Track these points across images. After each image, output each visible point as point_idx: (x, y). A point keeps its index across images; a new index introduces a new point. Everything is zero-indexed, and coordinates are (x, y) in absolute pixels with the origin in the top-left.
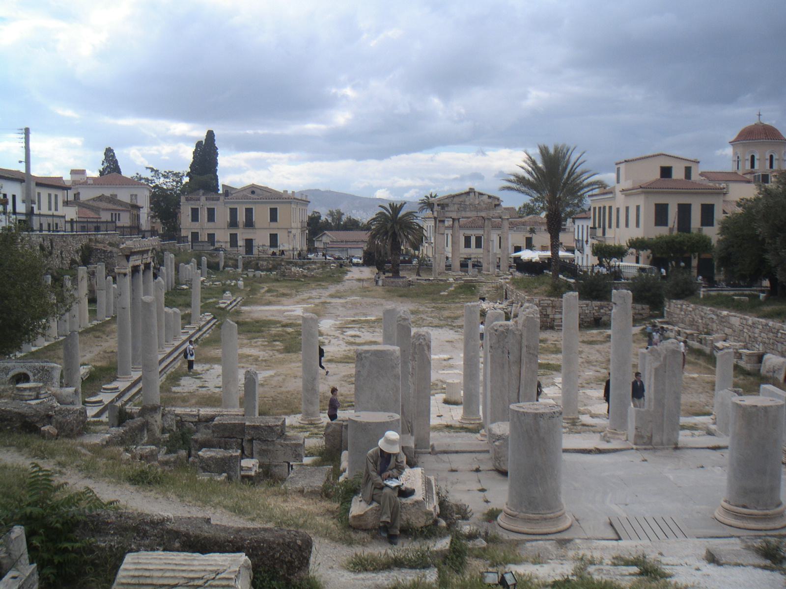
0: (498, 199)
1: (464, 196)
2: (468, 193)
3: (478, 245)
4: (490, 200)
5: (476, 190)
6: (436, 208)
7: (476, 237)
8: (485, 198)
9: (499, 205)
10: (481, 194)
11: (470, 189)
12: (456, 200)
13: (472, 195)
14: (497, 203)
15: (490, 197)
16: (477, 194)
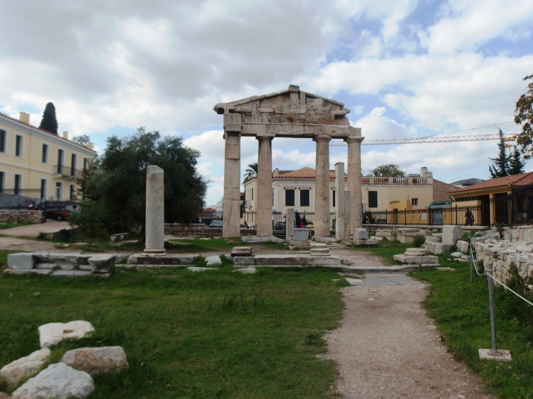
0: (341, 106)
1: (280, 100)
2: (286, 95)
3: (305, 201)
4: (327, 108)
5: (301, 89)
7: (301, 191)
8: (317, 103)
9: (340, 117)
10: (309, 96)
11: (292, 86)
12: (266, 108)
13: (294, 97)
14: (338, 112)
15: (326, 102)
16: (303, 97)
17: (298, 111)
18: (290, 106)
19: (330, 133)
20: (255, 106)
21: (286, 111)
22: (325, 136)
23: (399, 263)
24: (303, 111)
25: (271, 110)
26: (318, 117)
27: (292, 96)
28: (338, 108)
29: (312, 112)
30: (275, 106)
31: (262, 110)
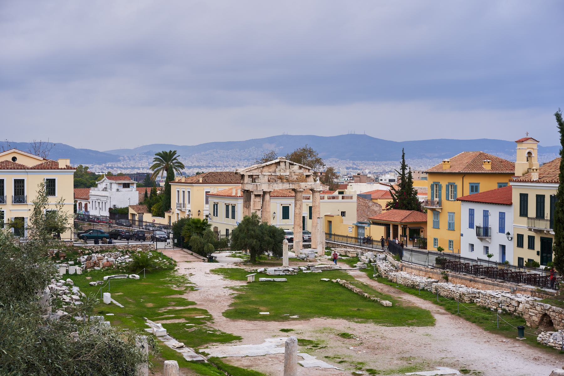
4: (301, 171)
6: (246, 179)
12: (266, 172)
13: (282, 164)
16: (288, 164)
17: (284, 174)
18: (280, 171)
19: (304, 188)
20: (260, 171)
21: (278, 174)
22: (301, 190)
23: (356, 267)
24: (288, 174)
25: (270, 174)
26: (296, 177)
27: (281, 164)
28: (307, 171)
29: (293, 174)
30: (270, 170)
31: (264, 174)
